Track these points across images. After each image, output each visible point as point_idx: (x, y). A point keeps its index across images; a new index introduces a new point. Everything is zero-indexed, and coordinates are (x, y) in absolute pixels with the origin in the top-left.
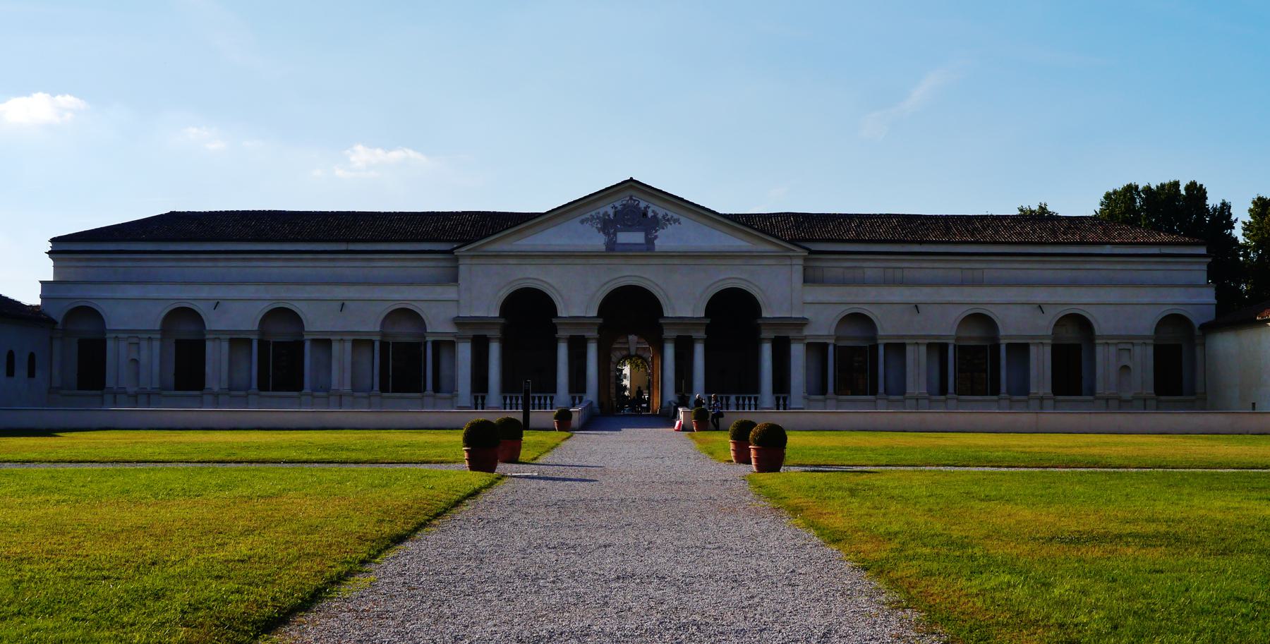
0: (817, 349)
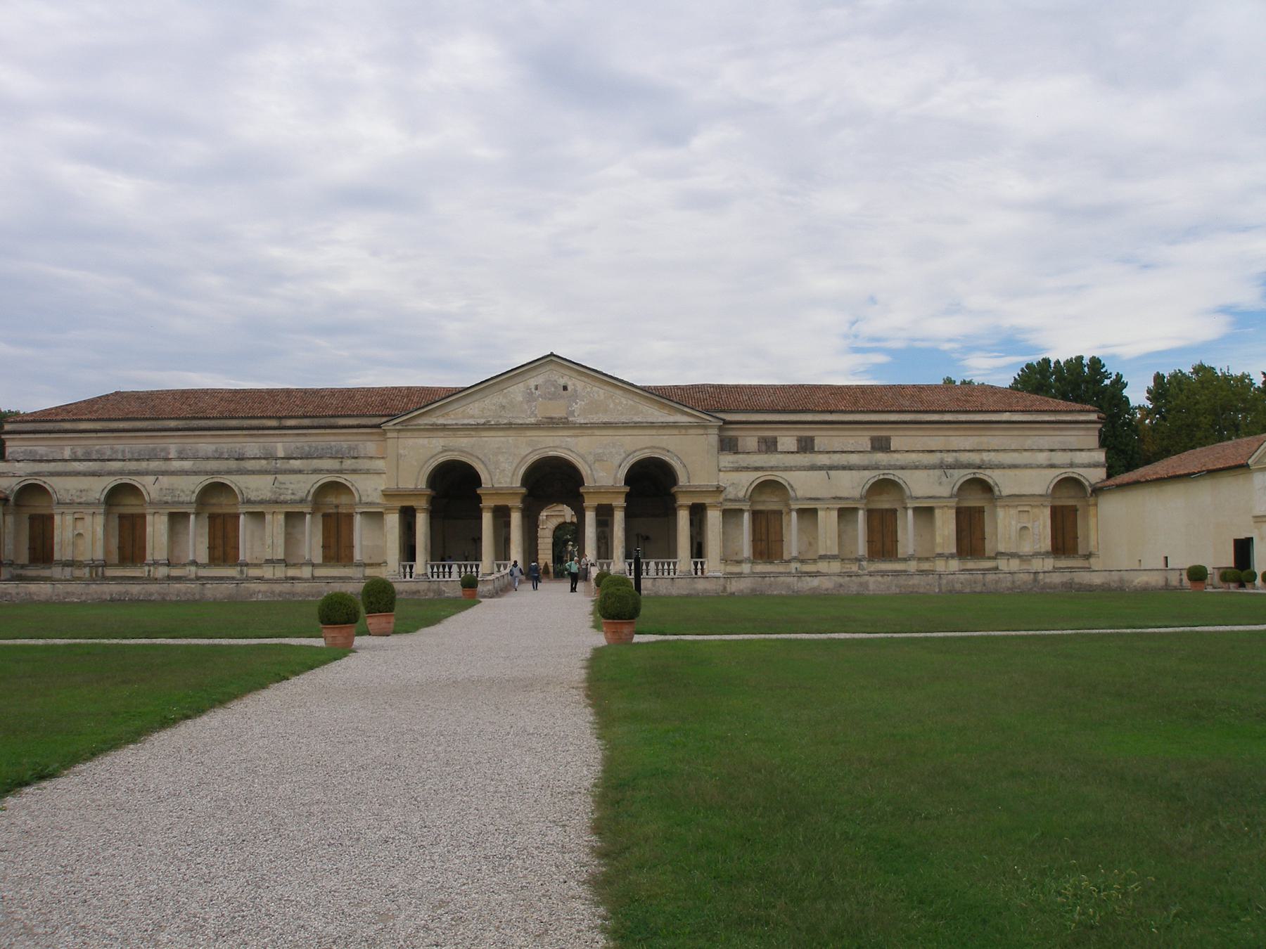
0: (730, 515)
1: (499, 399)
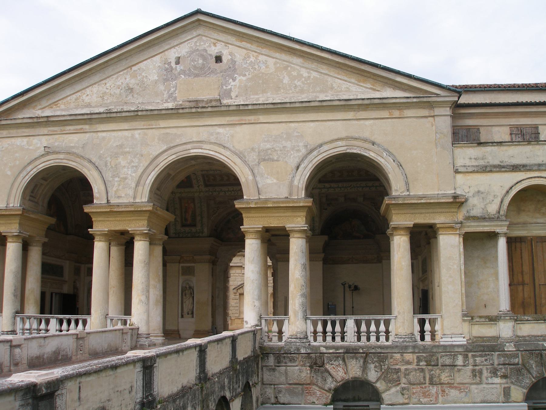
1: (126, 79)
